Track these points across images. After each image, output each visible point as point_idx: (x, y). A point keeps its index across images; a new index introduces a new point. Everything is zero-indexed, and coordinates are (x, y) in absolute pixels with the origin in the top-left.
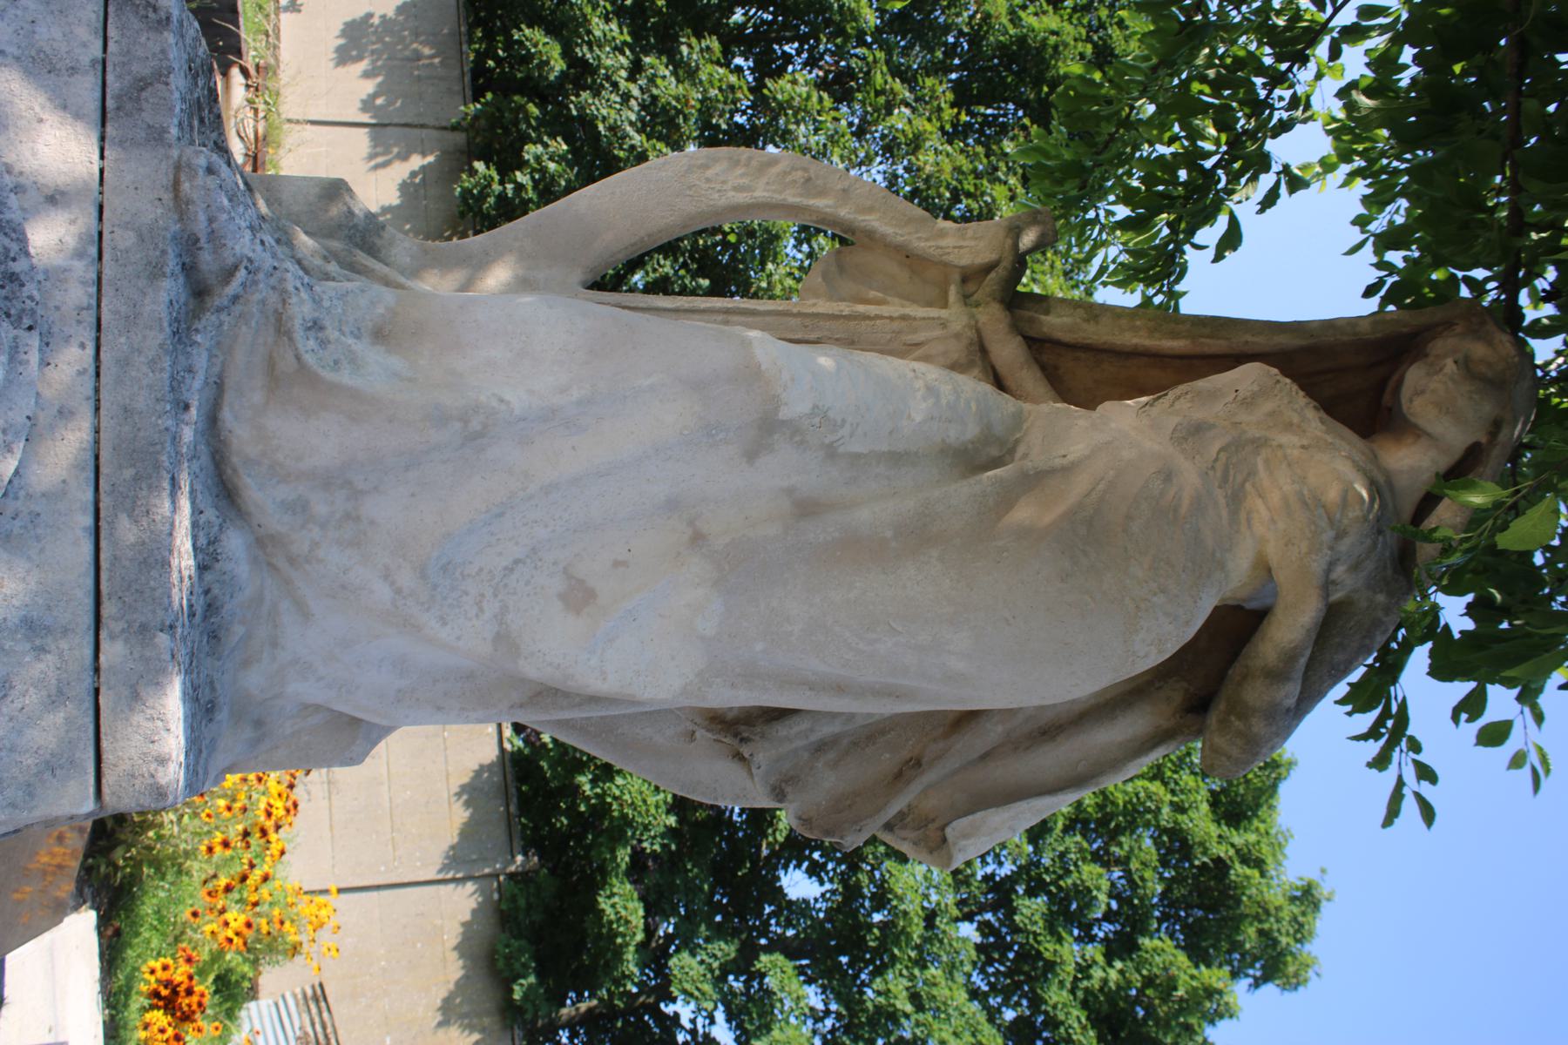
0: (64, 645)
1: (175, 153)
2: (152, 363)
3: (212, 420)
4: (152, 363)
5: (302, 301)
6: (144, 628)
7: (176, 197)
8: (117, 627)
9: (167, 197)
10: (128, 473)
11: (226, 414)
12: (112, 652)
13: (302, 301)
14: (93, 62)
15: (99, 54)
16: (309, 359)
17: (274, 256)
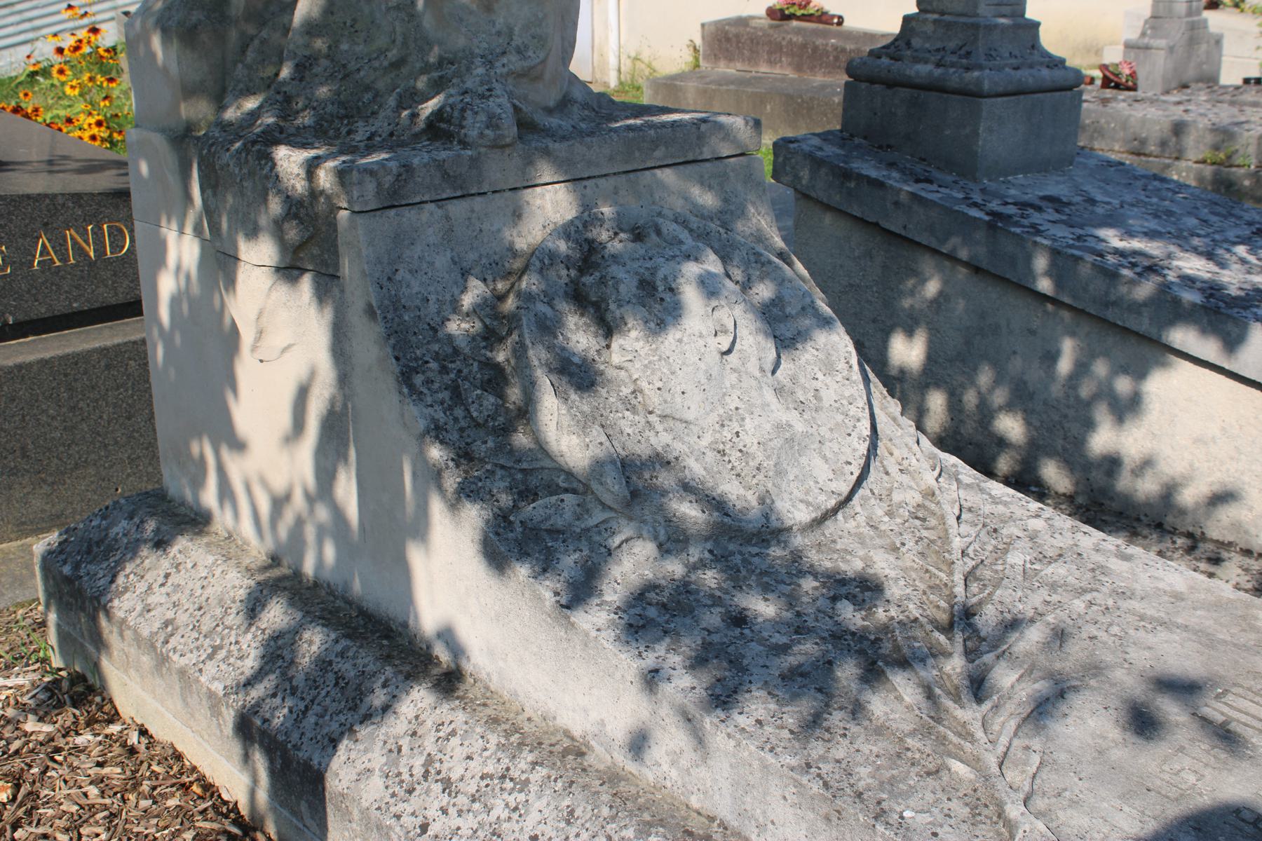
0: (706, 177)
1: (483, 150)
2: (589, 148)
3: (549, 111)
4: (589, 148)
5: (509, 61)
6: (699, 138)
7: (508, 145)
8: (698, 151)
9: (507, 151)
10: (637, 154)
11: (552, 104)
12: (707, 155)
13: (509, 61)
14: (439, 207)
15: (432, 206)
16: (542, 55)
17: (489, 82)
